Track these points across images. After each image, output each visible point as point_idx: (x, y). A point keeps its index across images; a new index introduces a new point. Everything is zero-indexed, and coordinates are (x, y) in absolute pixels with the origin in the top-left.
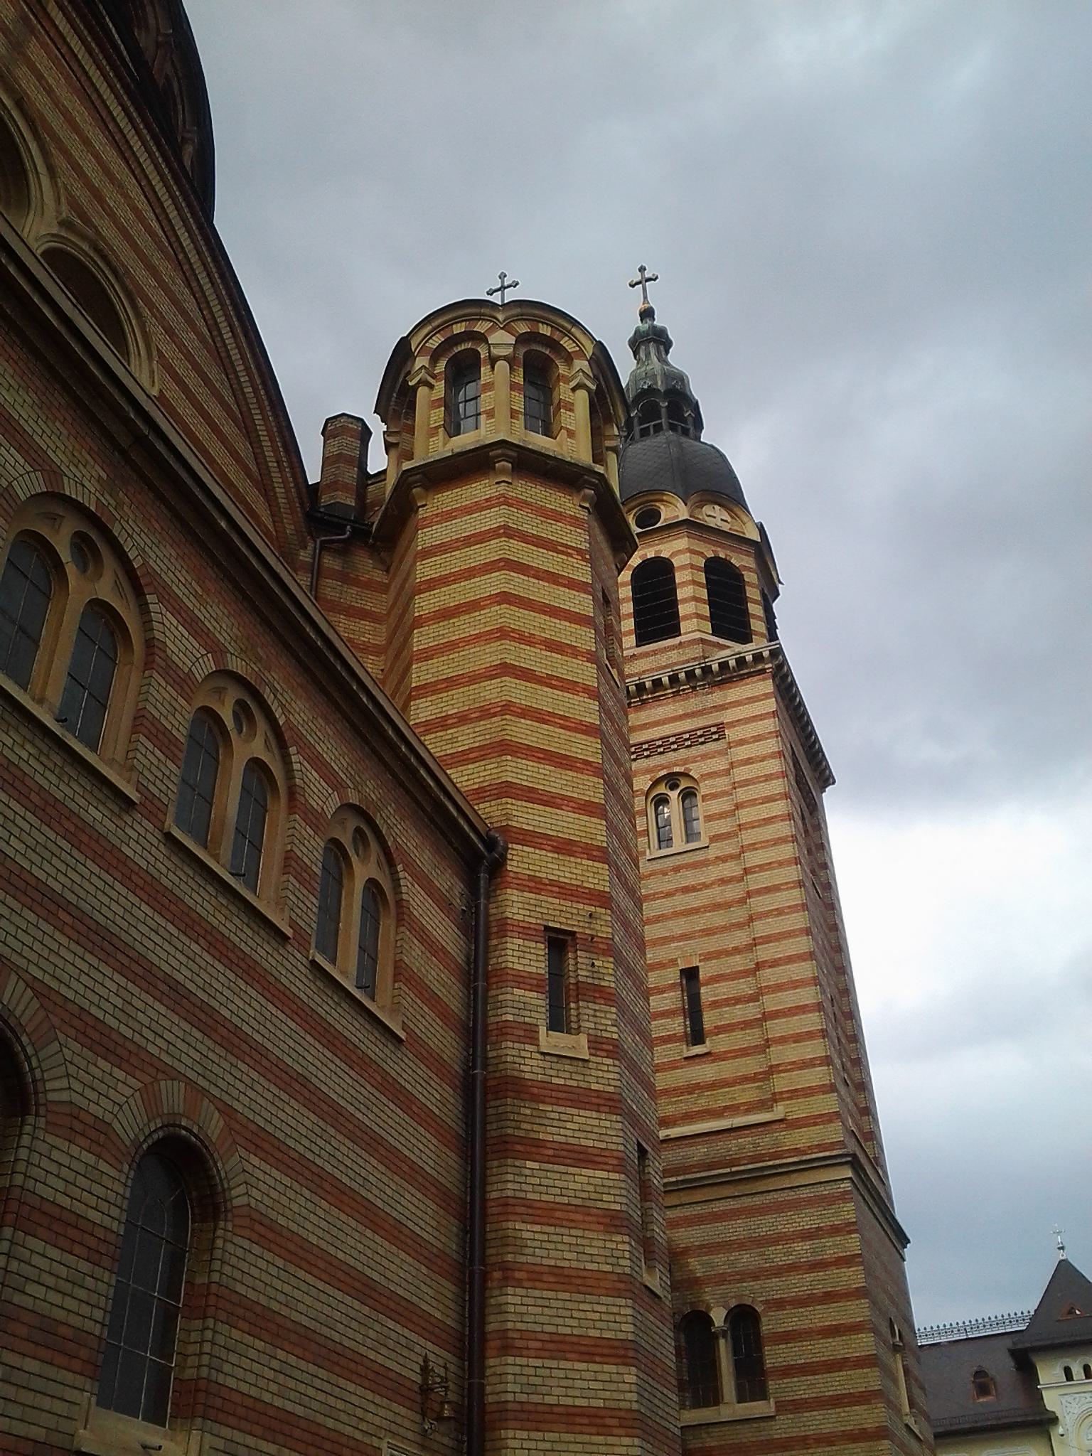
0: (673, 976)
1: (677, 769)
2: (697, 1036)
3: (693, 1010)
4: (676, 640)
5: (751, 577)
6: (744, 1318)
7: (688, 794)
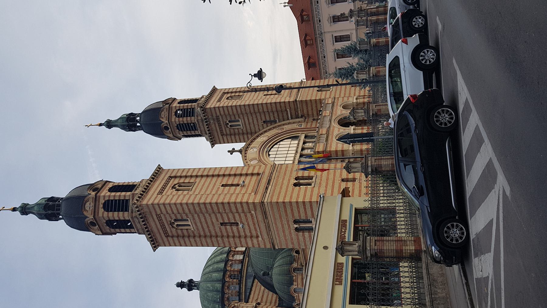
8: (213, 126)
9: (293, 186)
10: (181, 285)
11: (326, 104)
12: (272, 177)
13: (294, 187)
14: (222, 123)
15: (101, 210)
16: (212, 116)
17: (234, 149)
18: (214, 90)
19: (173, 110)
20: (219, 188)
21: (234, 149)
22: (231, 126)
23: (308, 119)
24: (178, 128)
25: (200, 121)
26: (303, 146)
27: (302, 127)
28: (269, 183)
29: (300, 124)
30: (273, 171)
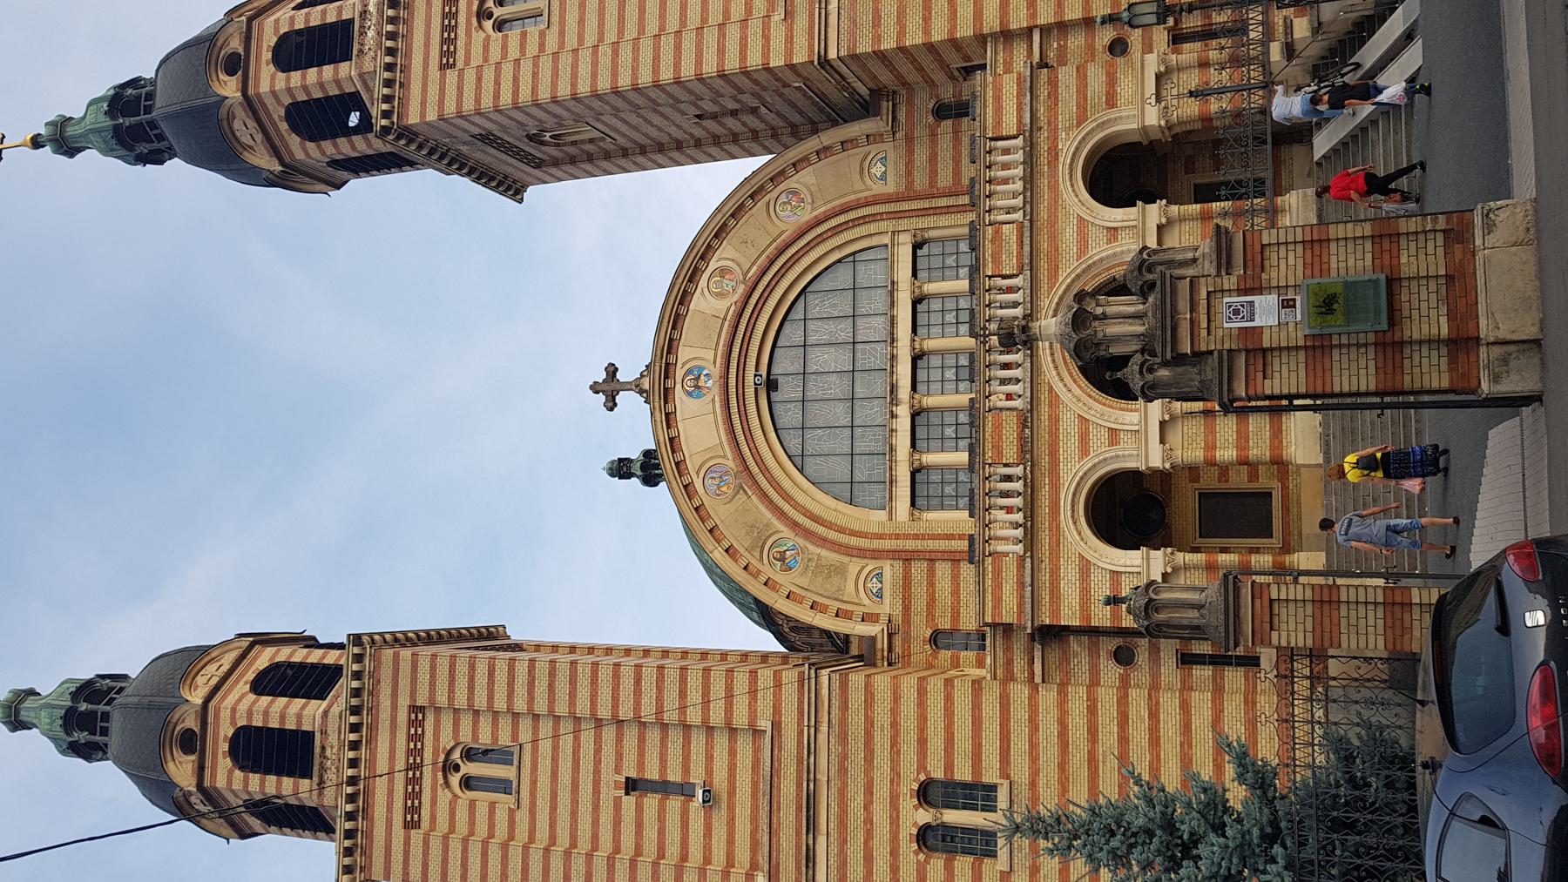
0: (629, 802)
1: (442, 758)
2: (685, 790)
3: (664, 788)
4: (318, 735)
5: (284, 654)
6: (925, 794)
7: (469, 755)
9: (916, 853)
10: (621, 469)
11: (991, 139)
12: (818, 776)
13: (922, 857)
17: (612, 370)
19: (271, 109)
20: (617, 803)
21: (612, 370)
23: (910, 102)
26: (917, 346)
27: (890, 188)
28: (811, 825)
29: (874, 149)
30: (812, 730)
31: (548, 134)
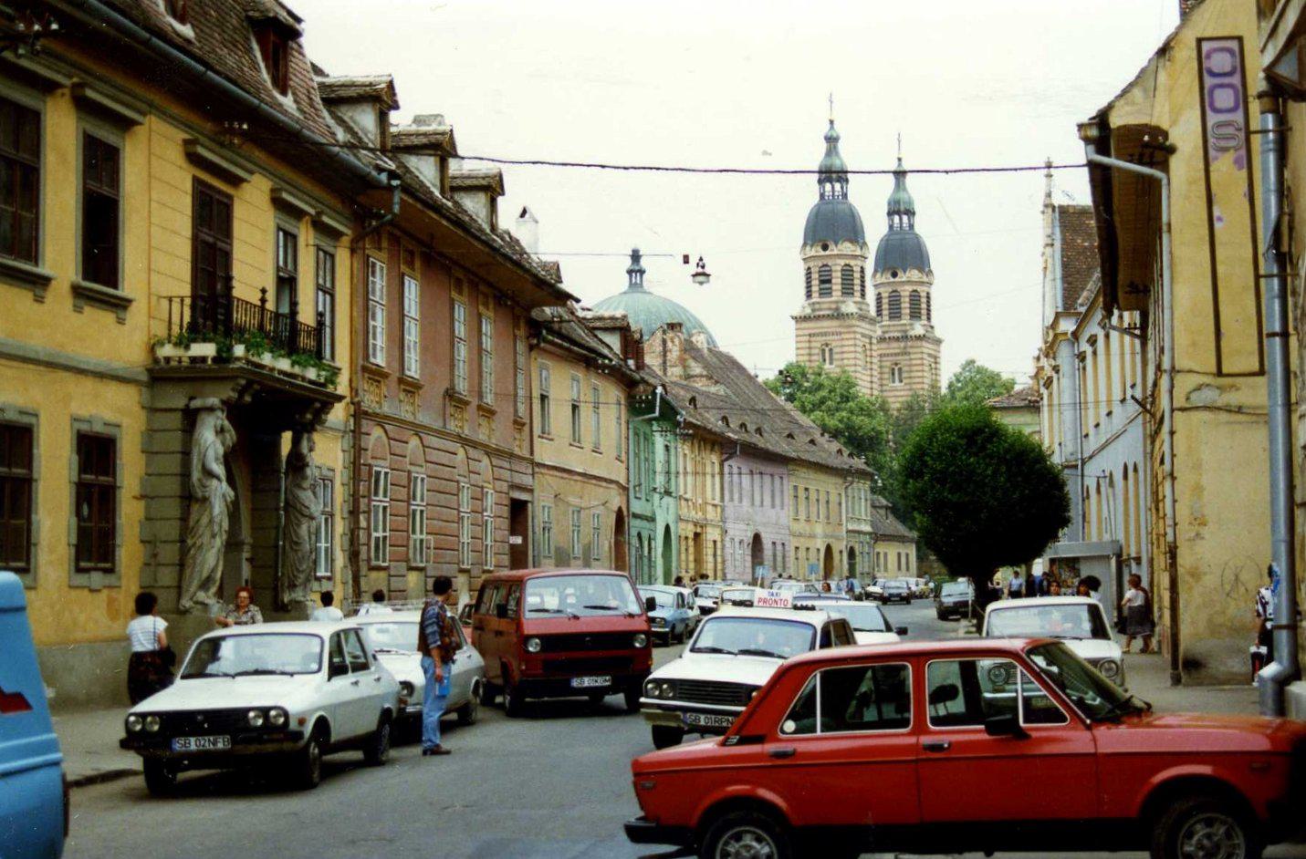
8: (895, 345)
14: (900, 358)
15: (842, 262)
16: (911, 347)
18: (938, 342)
22: (893, 369)
24: (894, 291)
25: (904, 328)
31: (896, 368)
